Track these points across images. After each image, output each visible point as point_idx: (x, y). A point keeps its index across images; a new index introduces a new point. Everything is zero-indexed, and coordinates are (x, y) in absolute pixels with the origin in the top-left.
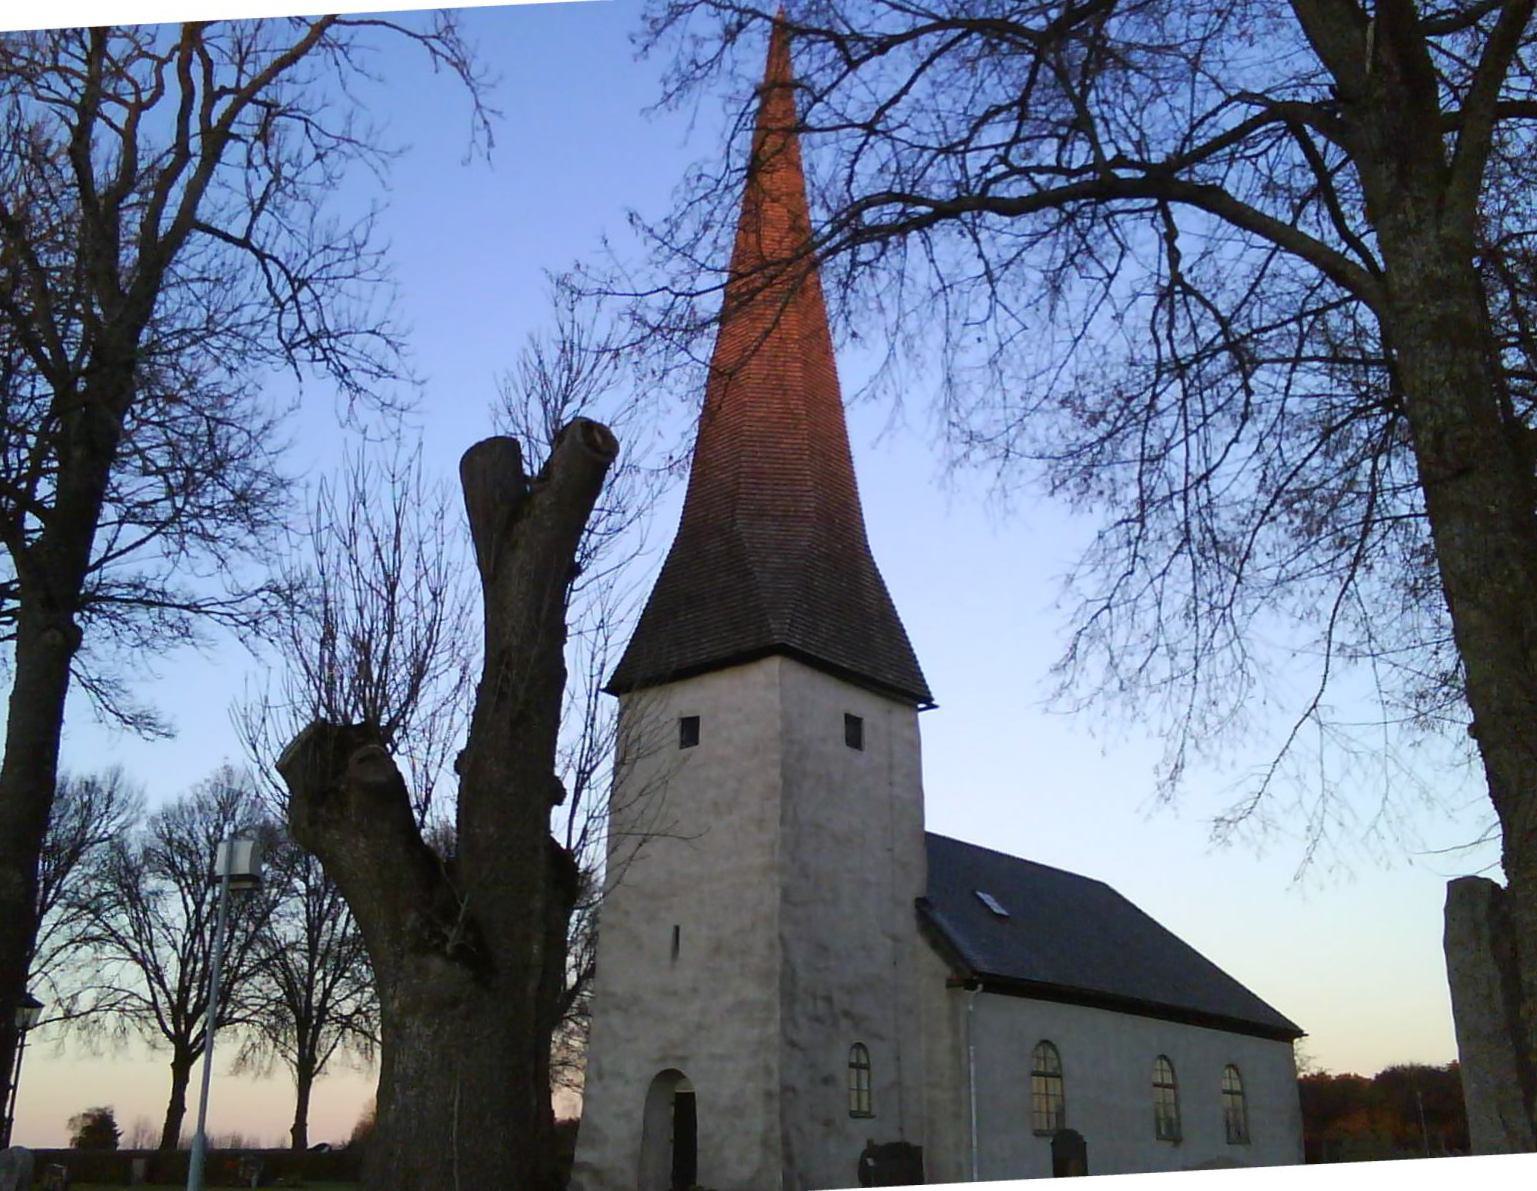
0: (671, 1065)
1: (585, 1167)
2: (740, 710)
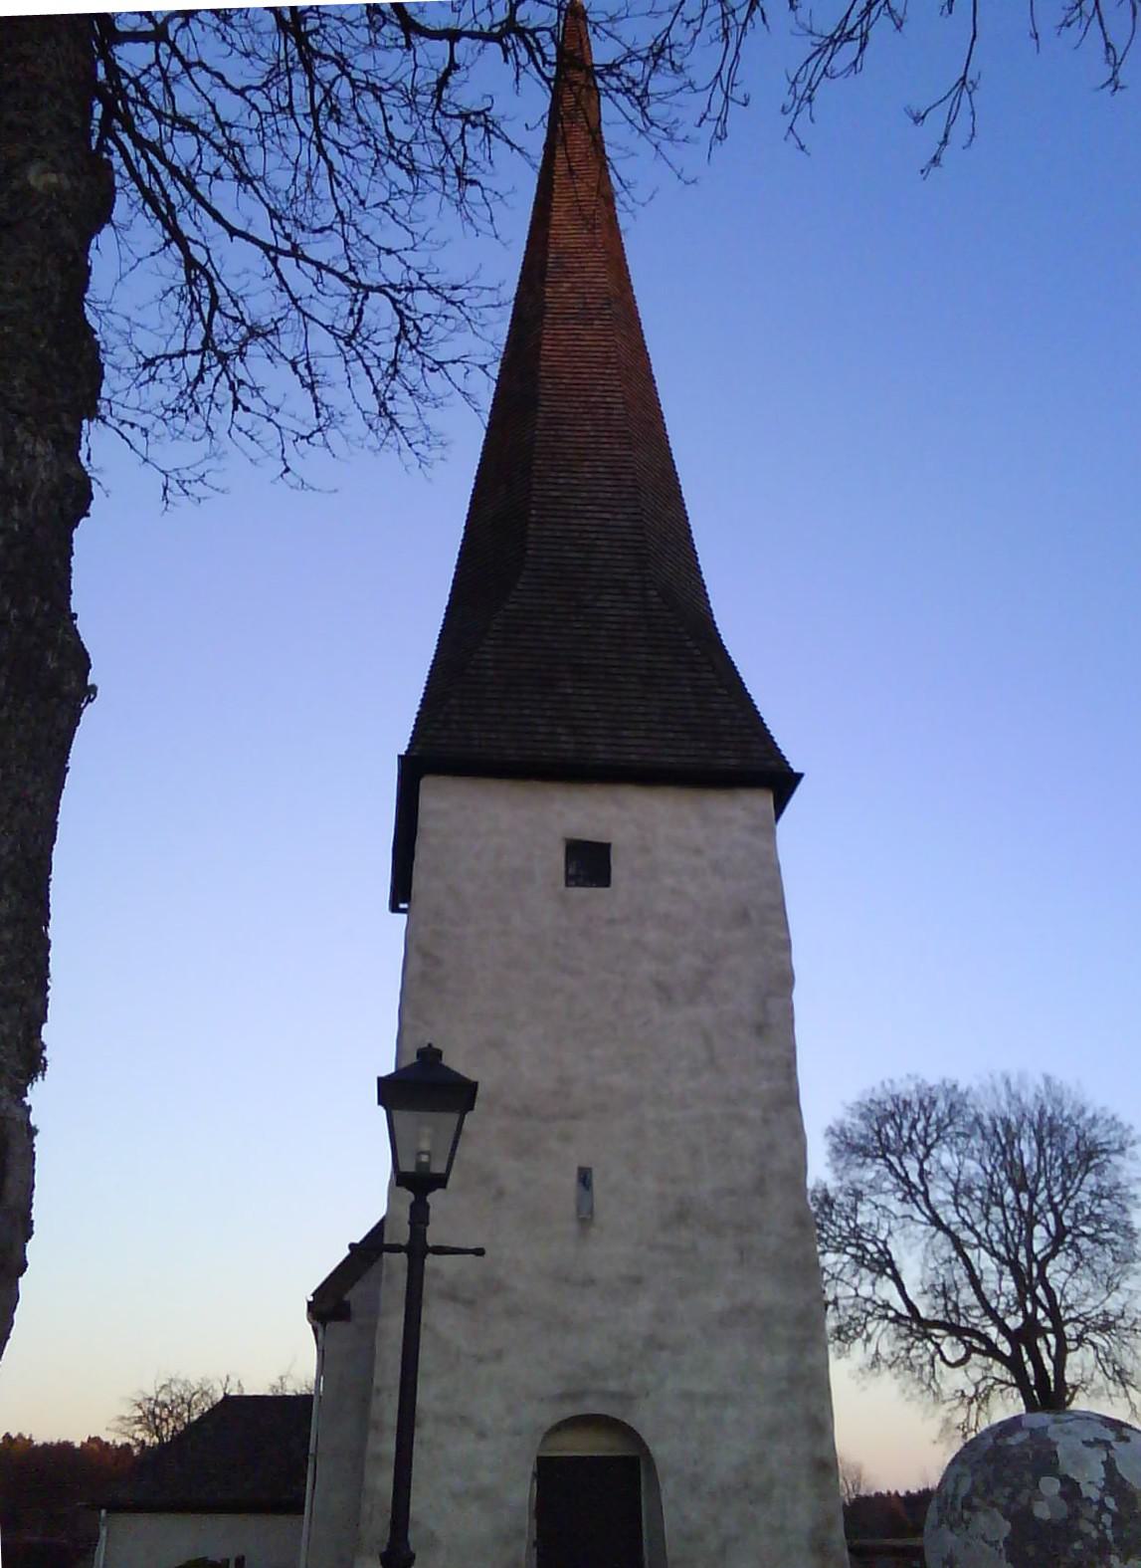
0: (592, 1406)
2: (698, 852)
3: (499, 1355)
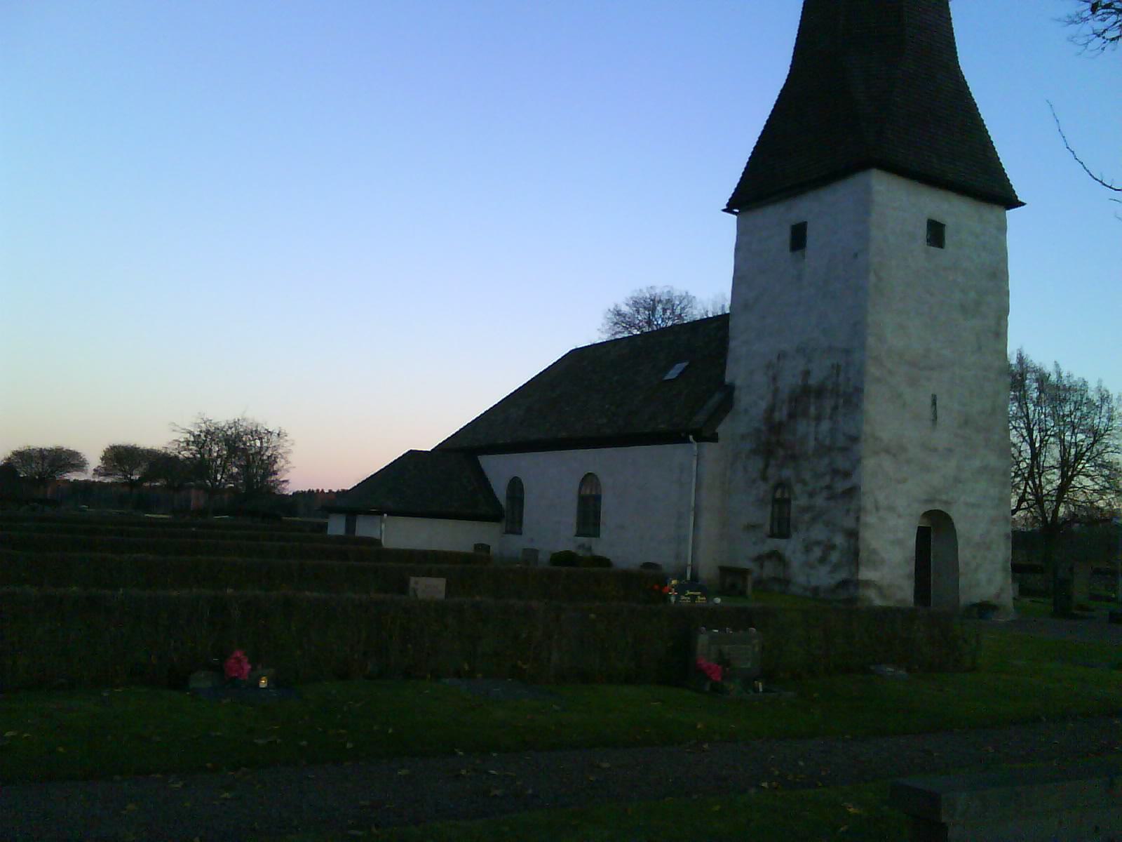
1: (868, 584)
3: (904, 481)
